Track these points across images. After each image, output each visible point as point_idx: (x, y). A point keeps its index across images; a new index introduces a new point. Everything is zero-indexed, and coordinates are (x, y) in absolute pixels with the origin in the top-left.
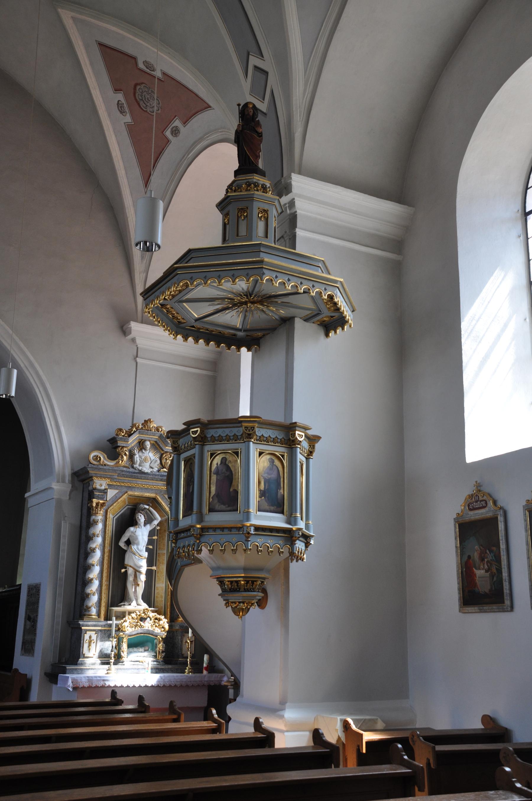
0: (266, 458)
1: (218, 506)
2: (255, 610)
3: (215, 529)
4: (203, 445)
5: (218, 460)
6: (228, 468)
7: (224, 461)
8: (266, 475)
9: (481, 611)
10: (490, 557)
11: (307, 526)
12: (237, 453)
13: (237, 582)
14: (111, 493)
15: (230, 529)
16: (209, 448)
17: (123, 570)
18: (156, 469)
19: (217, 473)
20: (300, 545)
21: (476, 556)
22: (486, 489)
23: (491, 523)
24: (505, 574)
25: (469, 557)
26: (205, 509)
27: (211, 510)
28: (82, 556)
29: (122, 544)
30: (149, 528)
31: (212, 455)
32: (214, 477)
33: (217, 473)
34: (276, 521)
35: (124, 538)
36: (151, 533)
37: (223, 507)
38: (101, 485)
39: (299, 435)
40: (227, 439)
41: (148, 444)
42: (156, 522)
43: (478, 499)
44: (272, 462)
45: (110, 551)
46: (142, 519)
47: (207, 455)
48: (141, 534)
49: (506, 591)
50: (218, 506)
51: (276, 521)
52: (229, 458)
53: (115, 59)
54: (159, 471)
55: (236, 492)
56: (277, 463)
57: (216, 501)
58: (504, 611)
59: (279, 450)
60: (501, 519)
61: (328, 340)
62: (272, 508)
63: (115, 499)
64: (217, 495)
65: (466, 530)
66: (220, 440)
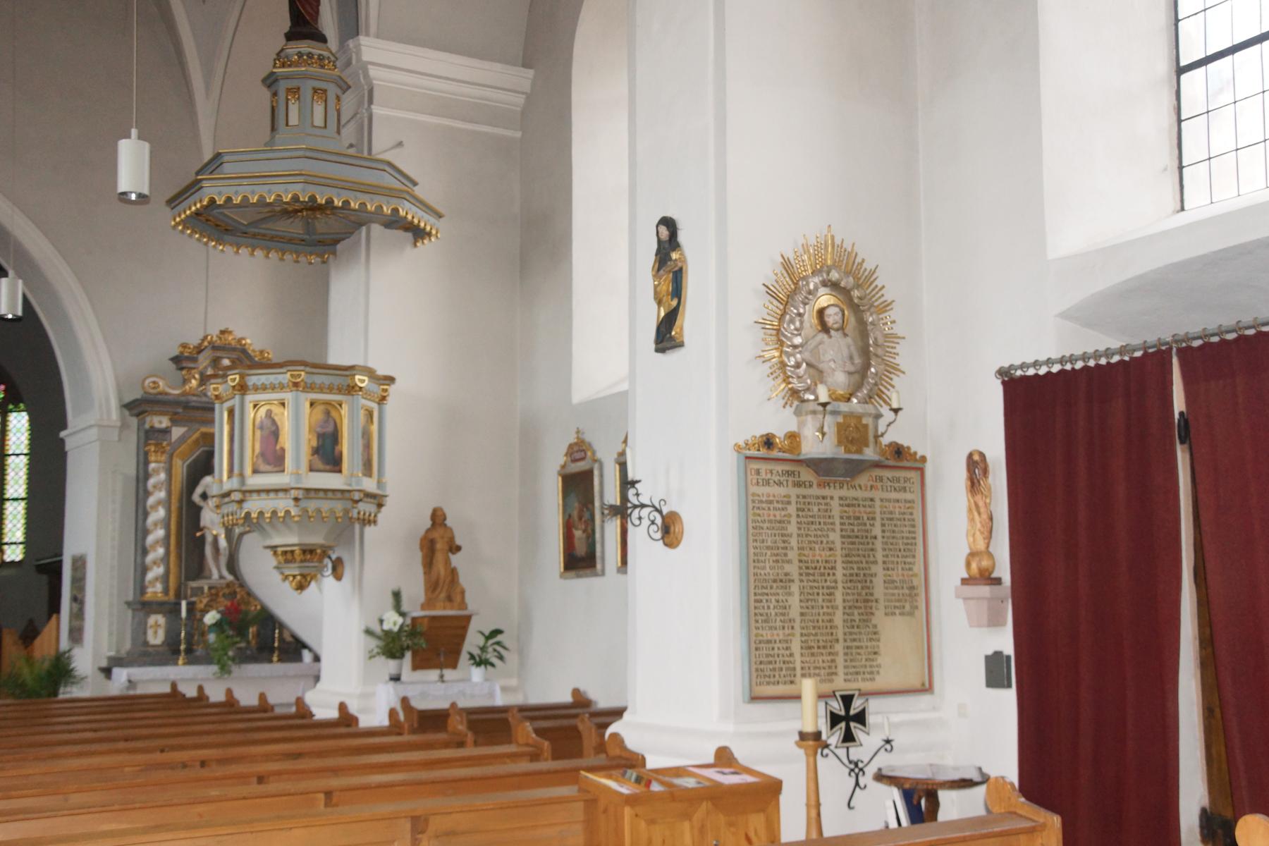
0: (319, 409)
1: (263, 467)
2: (328, 581)
3: (259, 492)
4: (243, 394)
5: (262, 412)
6: (274, 422)
7: (269, 413)
8: (319, 430)
9: (579, 576)
10: (587, 515)
11: (380, 484)
12: (283, 404)
13: (292, 552)
14: (177, 432)
15: (276, 491)
16: (250, 398)
17: (198, 534)
21: (575, 514)
22: (588, 437)
23: (587, 476)
24: (598, 535)
26: (248, 470)
27: (255, 471)
28: (141, 517)
29: (196, 497)
31: (255, 406)
32: (258, 433)
33: (261, 428)
35: (199, 490)
37: (269, 468)
38: (160, 422)
40: (273, 388)
43: (579, 449)
44: (328, 413)
45: (180, 509)
49: (598, 554)
50: (263, 467)
52: (276, 410)
55: (283, 450)
57: (260, 461)
58: (596, 575)
60: (596, 473)
61: (416, 250)
62: (328, 467)
63: (183, 439)
64: (262, 454)
66: (264, 388)
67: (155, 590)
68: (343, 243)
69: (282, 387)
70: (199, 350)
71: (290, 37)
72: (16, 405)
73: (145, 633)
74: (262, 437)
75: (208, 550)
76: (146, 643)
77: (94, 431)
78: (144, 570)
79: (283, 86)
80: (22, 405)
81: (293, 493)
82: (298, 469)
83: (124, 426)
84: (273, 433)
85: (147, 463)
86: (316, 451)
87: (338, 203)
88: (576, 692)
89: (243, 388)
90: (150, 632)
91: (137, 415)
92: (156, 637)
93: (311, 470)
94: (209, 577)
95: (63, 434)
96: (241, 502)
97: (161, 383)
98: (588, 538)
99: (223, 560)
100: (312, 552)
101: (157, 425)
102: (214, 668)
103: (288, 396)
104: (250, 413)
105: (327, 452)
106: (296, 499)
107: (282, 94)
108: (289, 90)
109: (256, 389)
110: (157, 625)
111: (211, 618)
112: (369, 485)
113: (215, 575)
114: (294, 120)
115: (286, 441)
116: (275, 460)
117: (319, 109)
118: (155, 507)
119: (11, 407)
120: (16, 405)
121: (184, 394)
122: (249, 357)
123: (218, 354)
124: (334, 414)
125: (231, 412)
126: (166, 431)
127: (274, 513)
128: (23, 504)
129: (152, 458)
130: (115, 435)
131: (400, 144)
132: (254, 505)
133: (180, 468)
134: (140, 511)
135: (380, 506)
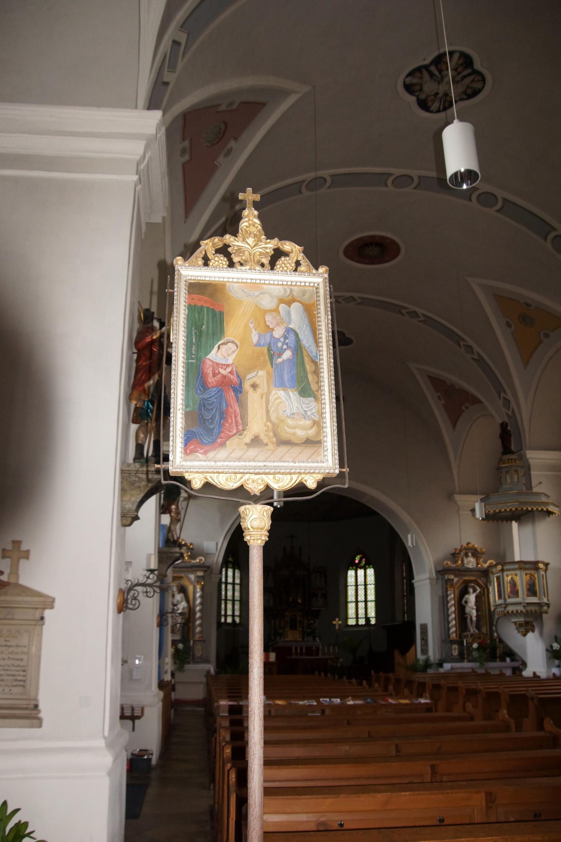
0: (528, 576)
5: (509, 578)
6: (514, 581)
7: (512, 578)
11: (548, 600)
14: (456, 580)
16: (505, 573)
18: (475, 566)
19: (510, 582)
20: (545, 608)
26: (507, 597)
27: (509, 597)
29: (463, 602)
30: (474, 595)
32: (509, 585)
34: (534, 600)
35: (464, 600)
39: (541, 566)
40: (513, 570)
41: (470, 554)
42: (478, 592)
44: (531, 577)
46: (471, 590)
47: (505, 576)
48: (472, 598)
50: (511, 596)
51: (534, 600)
52: (514, 577)
53: (437, 383)
54: (477, 566)
55: (518, 590)
56: (533, 577)
59: (532, 572)
63: (457, 582)
64: (511, 592)
66: (510, 570)
67: (453, 636)
69: (515, 569)
70: (461, 550)
71: (504, 453)
72: (369, 566)
73: (452, 652)
74: (510, 586)
75: (469, 621)
76: (452, 655)
78: (449, 629)
80: (371, 566)
81: (523, 604)
82: (523, 597)
83: (437, 579)
84: (513, 584)
85: (447, 591)
86: (529, 590)
87: (530, 509)
89: (502, 570)
90: (453, 651)
91: (442, 575)
92: (455, 653)
93: (528, 596)
94: (470, 631)
95: (413, 581)
96: (505, 608)
97: (449, 563)
99: (474, 625)
103: (518, 572)
104: (506, 578)
105: (532, 591)
106: (524, 606)
109: (507, 570)
110: (455, 649)
111: (475, 646)
112: (545, 600)
113: (472, 630)
115: (519, 588)
116: (515, 593)
117: (516, 477)
118: (451, 607)
119: (367, 567)
120: (369, 566)
121: (457, 566)
122: (478, 552)
123: (467, 551)
124: (533, 577)
125: (498, 578)
126: (452, 580)
127: (517, 611)
128: (374, 603)
129: (449, 589)
130: (435, 581)
131: (540, 483)
132: (510, 609)
133: (457, 592)
134: (445, 609)
135: (549, 607)
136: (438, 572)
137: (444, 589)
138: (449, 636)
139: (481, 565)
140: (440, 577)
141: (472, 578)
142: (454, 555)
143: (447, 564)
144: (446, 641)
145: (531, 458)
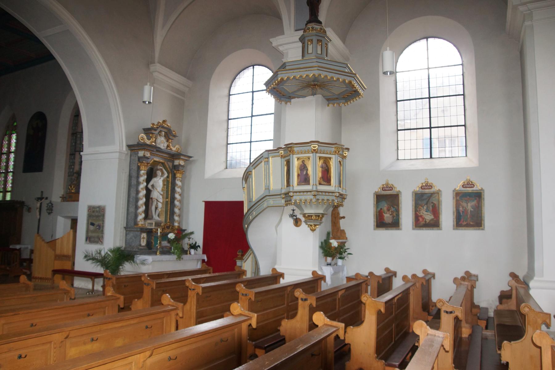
1: (322, 183)
6: (327, 166)
21: (385, 209)
25: (381, 209)
30: (162, 179)
35: (151, 183)
36: (163, 181)
37: (325, 183)
46: (159, 173)
50: (322, 183)
65: (379, 198)
68: (296, 100)
71: (309, 22)
73: (140, 241)
75: (153, 208)
76: (140, 245)
77: (118, 154)
79: (307, 39)
88: (387, 270)
90: (142, 240)
92: (144, 243)
95: (82, 153)
98: (393, 217)
100: (319, 216)
101: (146, 155)
102: (175, 257)
107: (306, 41)
108: (309, 40)
110: (143, 238)
114: (310, 51)
123: (162, 129)
136: (129, 146)
137: (135, 167)
138: (136, 223)
139: (171, 149)
140: (130, 151)
141: (161, 161)
142: (148, 131)
143: (143, 139)
144: (131, 226)
145: (281, 45)
